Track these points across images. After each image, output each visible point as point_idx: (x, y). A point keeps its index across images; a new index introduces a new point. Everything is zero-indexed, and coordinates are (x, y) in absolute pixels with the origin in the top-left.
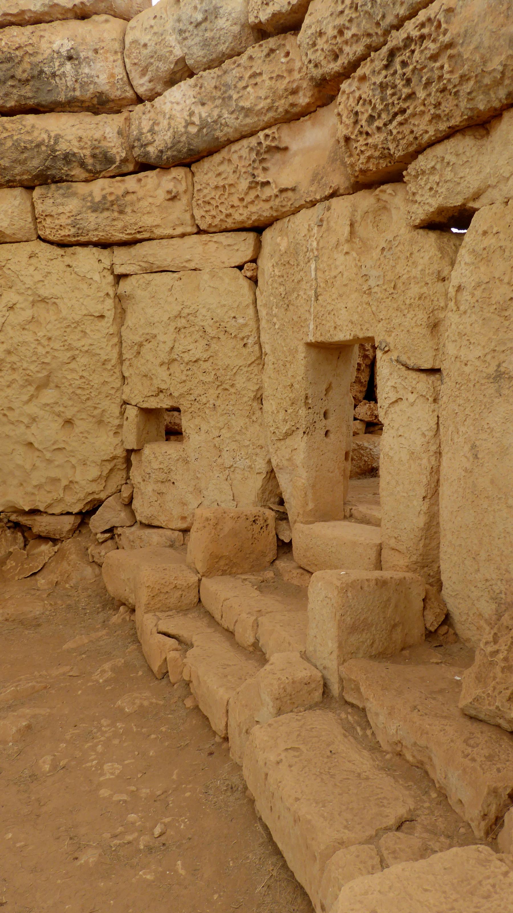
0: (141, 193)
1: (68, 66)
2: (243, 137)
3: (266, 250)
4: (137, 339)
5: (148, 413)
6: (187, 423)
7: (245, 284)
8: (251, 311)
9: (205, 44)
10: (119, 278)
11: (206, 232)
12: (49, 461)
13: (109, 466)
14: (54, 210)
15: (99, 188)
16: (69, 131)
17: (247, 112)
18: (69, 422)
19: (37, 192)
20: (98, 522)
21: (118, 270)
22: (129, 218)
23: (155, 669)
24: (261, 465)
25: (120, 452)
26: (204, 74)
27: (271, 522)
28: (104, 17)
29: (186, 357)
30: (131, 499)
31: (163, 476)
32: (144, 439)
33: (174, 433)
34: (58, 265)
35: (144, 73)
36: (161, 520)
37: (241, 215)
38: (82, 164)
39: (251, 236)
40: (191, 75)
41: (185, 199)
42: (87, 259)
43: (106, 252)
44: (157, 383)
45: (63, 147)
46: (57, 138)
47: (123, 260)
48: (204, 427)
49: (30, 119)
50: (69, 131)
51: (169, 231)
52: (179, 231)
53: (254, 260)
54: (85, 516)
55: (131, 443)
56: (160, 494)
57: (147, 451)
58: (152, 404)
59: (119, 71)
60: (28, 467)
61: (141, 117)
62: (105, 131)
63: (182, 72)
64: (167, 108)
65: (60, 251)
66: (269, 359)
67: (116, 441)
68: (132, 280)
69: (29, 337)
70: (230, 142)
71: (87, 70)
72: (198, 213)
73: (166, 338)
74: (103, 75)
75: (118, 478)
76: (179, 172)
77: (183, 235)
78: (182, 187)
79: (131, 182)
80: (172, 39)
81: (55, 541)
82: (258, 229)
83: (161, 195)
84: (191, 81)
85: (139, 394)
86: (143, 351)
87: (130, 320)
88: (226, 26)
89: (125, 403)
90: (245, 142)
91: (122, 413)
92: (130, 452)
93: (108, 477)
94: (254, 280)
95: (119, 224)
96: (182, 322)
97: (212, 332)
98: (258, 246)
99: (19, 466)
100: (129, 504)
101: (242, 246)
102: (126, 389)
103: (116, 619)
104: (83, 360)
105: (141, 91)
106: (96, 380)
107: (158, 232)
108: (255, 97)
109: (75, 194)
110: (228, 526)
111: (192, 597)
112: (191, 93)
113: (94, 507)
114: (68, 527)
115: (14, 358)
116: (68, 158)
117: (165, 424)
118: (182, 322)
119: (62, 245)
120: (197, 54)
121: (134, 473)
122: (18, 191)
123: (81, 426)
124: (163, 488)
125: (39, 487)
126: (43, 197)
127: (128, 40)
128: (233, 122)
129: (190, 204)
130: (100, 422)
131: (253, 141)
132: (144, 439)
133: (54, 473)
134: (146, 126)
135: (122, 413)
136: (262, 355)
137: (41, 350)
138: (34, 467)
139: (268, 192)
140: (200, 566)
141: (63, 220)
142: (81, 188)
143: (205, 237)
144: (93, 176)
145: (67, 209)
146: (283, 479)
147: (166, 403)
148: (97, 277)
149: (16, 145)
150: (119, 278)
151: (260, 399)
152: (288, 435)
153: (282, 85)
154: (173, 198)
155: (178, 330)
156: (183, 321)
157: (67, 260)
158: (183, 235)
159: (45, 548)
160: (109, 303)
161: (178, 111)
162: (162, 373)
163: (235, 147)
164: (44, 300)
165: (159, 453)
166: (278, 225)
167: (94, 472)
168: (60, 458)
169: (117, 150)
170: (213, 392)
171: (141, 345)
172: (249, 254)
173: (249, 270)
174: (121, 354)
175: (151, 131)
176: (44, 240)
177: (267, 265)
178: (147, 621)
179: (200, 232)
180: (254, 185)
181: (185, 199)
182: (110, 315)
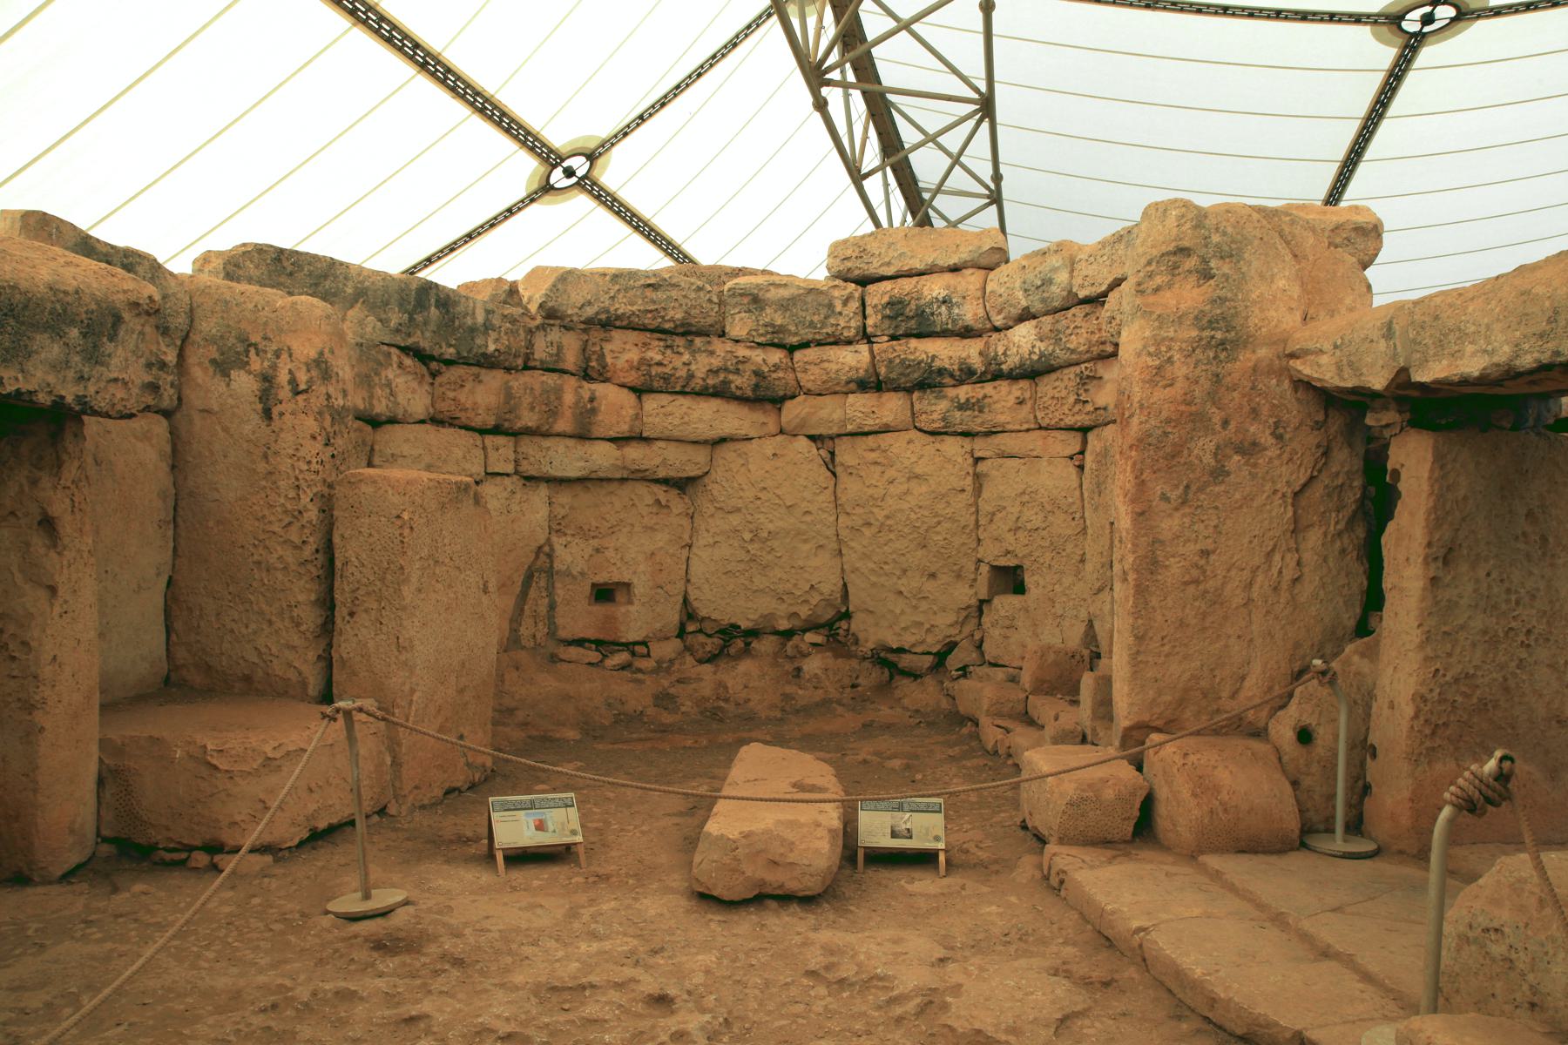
0: (996, 398)
1: (943, 308)
2: (1071, 365)
3: (1089, 447)
4: (990, 509)
5: (998, 570)
6: (1029, 580)
7: (1073, 471)
8: (1077, 493)
9: (1043, 300)
10: (977, 460)
11: (1046, 429)
12: (915, 608)
13: (964, 613)
14: (929, 409)
15: (964, 392)
16: (944, 352)
17: (1073, 351)
18: (933, 576)
19: (916, 395)
20: (954, 661)
21: (978, 454)
22: (986, 416)
23: (989, 747)
24: (1083, 614)
25: (974, 602)
26: (1043, 319)
27: (1087, 659)
28: (970, 271)
29: (1029, 526)
30: (982, 641)
31: (1008, 623)
32: (994, 591)
33: (1020, 589)
34: (930, 449)
35: (999, 312)
36: (1005, 660)
37: (1069, 421)
38: (952, 376)
39: (1079, 436)
40: (1034, 317)
41: (1029, 404)
42: (952, 446)
43: (967, 440)
44: (1006, 545)
45: (937, 364)
46: (934, 357)
47: (981, 447)
48: (1042, 582)
49: (913, 343)
50: (944, 352)
51: (1017, 427)
52: (1025, 426)
53: (1082, 452)
54: (941, 658)
55: (983, 595)
56: (1006, 637)
57: (996, 601)
58: (1002, 562)
59: (981, 312)
60: (898, 611)
61: (998, 344)
62: (971, 352)
63: (1026, 316)
64: (1016, 339)
65: (931, 439)
66: (1090, 531)
67: (972, 592)
68: (989, 462)
69: (906, 506)
70: (1061, 367)
71: (956, 311)
72: (1040, 415)
73: (1015, 510)
74: (969, 313)
75: (972, 623)
76: (1024, 384)
77: (1028, 430)
78: (1027, 395)
79: (988, 388)
80: (1020, 294)
81: (915, 675)
82: (1084, 430)
83: (1012, 400)
84: (1034, 322)
85: (991, 553)
86: (996, 518)
87: (985, 495)
88: (1056, 292)
89: (980, 561)
90: (1072, 369)
91: (977, 569)
92: (982, 602)
93: (962, 624)
94: (1081, 468)
95: (979, 420)
96: (1026, 498)
97: (1049, 508)
98: (1085, 442)
99: (892, 611)
100: (979, 647)
101: (1073, 443)
102: (981, 549)
103: (965, 731)
104: (947, 525)
105: (997, 324)
106: (957, 541)
107: (1009, 427)
108: (1079, 341)
109: (945, 397)
110: (1051, 657)
111: (1020, 707)
112: (1033, 331)
113: (951, 646)
114: (927, 665)
115: (889, 522)
116: (941, 372)
117: (1010, 579)
118: (1026, 498)
119: (933, 433)
120: (1037, 306)
121: (986, 620)
122: (901, 394)
123: (944, 578)
124: (1009, 633)
125: (905, 629)
126: (920, 399)
127: (988, 290)
128: (1062, 356)
129: (1033, 408)
130: (959, 576)
131: (1077, 369)
132: (994, 591)
133: (920, 618)
134: (1000, 350)
135: (977, 569)
136: (1085, 528)
137: (913, 516)
138: (903, 612)
139: (1089, 408)
140: (1027, 686)
141: (935, 416)
142: (951, 392)
143: (1043, 433)
144: (961, 382)
145: (938, 408)
146: (1097, 624)
147: (1012, 562)
148: (960, 460)
149: (903, 361)
150: (977, 460)
151: (1082, 561)
152: (1100, 590)
153: (1095, 338)
154: (1021, 402)
155: (1023, 504)
156: (1027, 497)
157: (938, 446)
158: (1028, 430)
159: (906, 681)
160: (969, 480)
161: (1023, 341)
162: (1010, 537)
163: (1066, 371)
164: (917, 477)
165: (1006, 604)
166: (1095, 431)
167: (952, 618)
168: (924, 605)
169: (977, 363)
170: (1048, 555)
171: (994, 514)
172: (1078, 448)
173: (1078, 460)
174: (977, 521)
175: (1004, 354)
176: (920, 430)
177: (1089, 459)
178: (985, 721)
179: (1040, 428)
180: (1077, 401)
181: (1029, 404)
182: (969, 489)
